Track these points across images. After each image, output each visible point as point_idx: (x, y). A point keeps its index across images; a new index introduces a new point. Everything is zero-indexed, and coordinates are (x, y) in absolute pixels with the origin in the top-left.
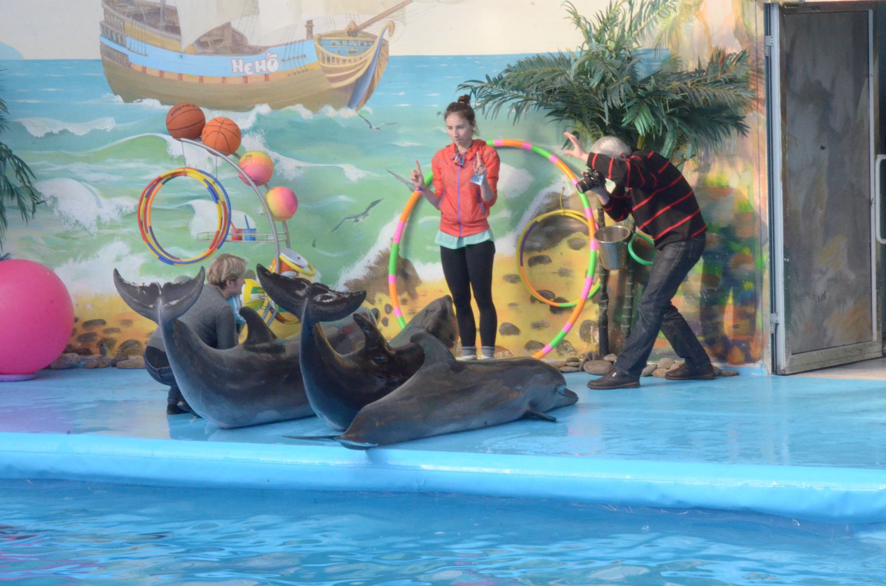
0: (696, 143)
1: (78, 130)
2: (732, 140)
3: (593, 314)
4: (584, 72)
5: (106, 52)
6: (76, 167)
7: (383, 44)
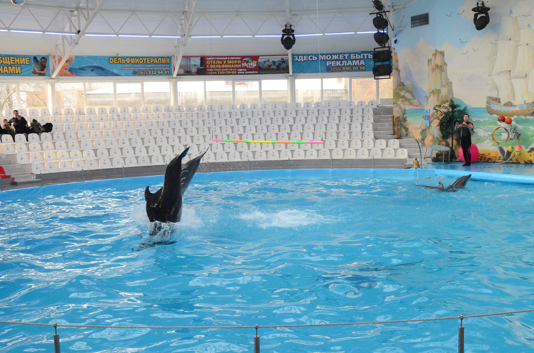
1: (481, 120)
5: (487, 106)
6: (481, 127)
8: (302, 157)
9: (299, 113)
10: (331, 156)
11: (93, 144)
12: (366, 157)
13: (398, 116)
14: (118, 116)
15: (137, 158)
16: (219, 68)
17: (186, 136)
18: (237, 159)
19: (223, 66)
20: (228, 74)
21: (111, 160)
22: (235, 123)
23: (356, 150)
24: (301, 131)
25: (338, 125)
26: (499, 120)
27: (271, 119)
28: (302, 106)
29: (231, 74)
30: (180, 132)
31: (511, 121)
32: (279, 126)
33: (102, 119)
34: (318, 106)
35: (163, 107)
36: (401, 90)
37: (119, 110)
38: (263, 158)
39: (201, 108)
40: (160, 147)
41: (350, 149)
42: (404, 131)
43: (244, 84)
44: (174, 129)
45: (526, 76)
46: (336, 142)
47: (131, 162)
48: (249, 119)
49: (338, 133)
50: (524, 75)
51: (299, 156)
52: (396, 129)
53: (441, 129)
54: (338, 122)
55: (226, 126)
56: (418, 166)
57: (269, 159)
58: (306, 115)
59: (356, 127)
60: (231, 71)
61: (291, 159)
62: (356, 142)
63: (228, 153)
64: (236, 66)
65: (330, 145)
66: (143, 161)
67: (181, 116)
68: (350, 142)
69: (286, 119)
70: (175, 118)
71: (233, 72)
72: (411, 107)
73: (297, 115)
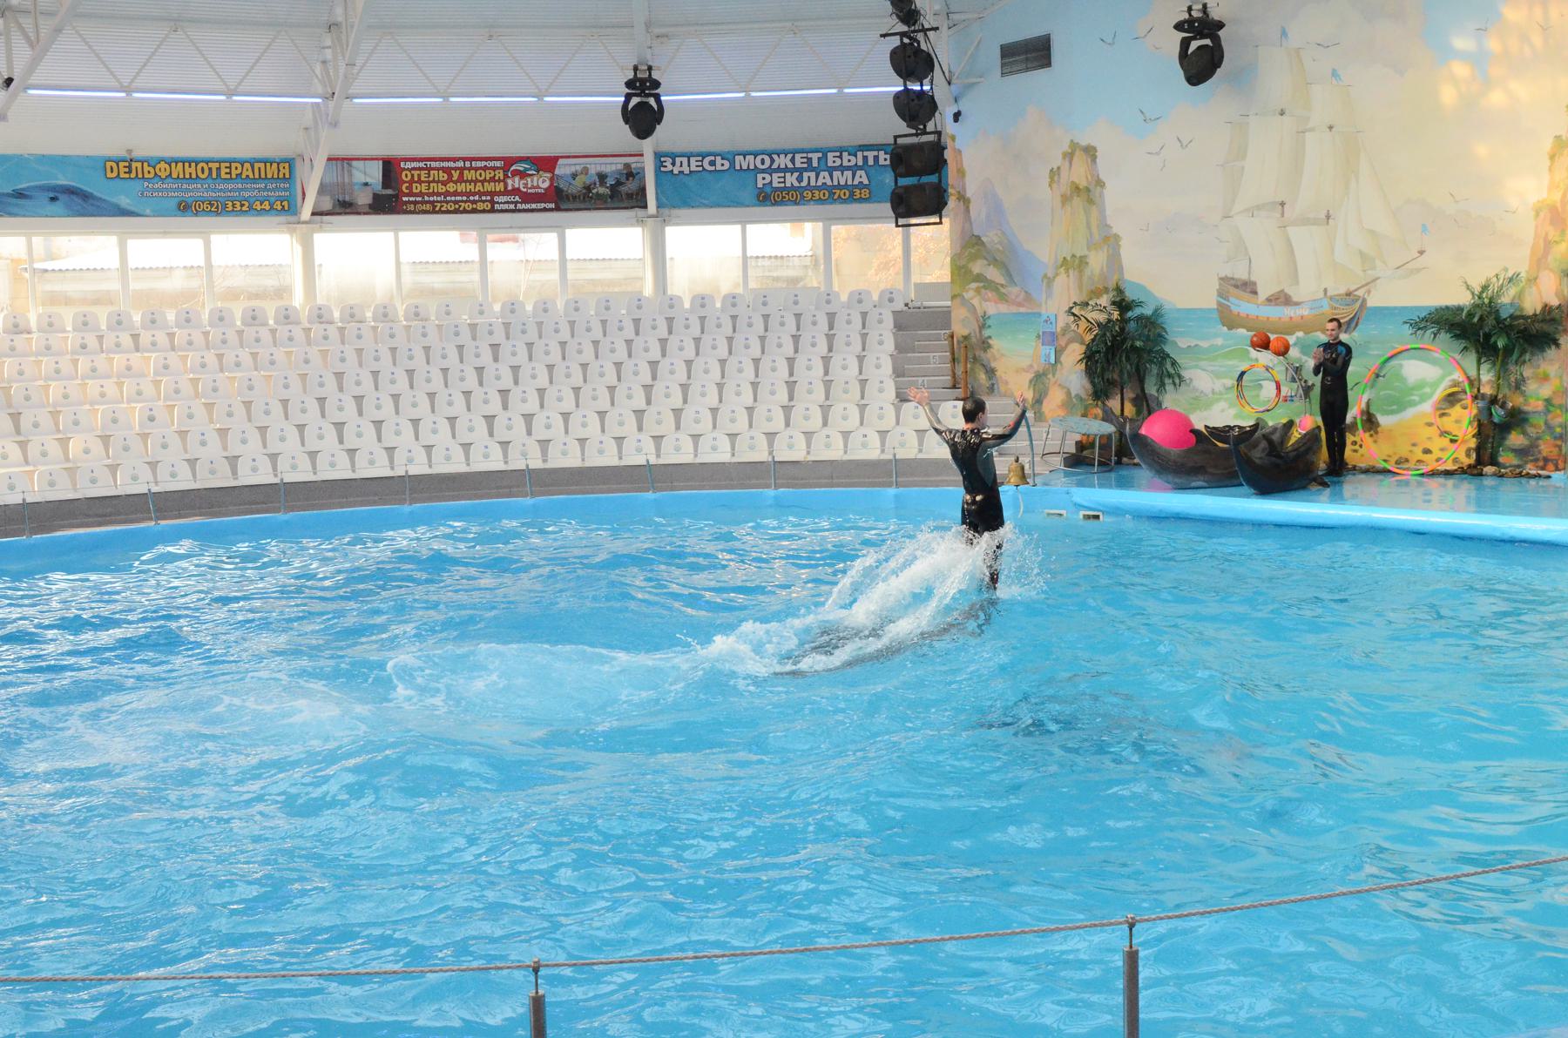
0: (1533, 354)
1: (1204, 344)
2: (1551, 352)
3: (1473, 443)
4: (1471, 315)
5: (1219, 304)
6: (1203, 363)
7: (1364, 300)
8: (687, 458)
9: (678, 325)
10: (771, 453)
11: (57, 424)
12: (873, 453)
13: (966, 333)
14: (135, 337)
15: (192, 463)
16: (439, 194)
17: (341, 396)
18: (495, 463)
19: (451, 187)
20: (465, 211)
21: (113, 469)
22: (486, 357)
23: (846, 435)
24: (684, 379)
25: (791, 361)
26: (1254, 345)
27: (596, 343)
28: (687, 305)
29: (474, 211)
30: (321, 385)
31: (1287, 349)
32: (618, 365)
33: (84, 347)
34: (734, 305)
35: (270, 309)
36: (973, 258)
37: (137, 318)
38: (572, 460)
39: (385, 314)
40: (263, 430)
41: (826, 431)
42: (982, 376)
43: (516, 240)
44: (303, 377)
45: (1328, 217)
46: (787, 410)
47: (173, 475)
48: (530, 345)
49: (791, 386)
50: (1323, 216)
51: (679, 452)
52: (960, 370)
53: (1090, 372)
54: (791, 353)
55: (461, 366)
56: (1023, 478)
57: (587, 464)
58: (697, 333)
59: (844, 368)
60: (474, 202)
61: (653, 461)
62: (846, 412)
63: (466, 447)
64: (489, 187)
65: (769, 420)
66: (213, 472)
67: (326, 338)
68: (825, 410)
69: (639, 343)
70: (309, 344)
71: (480, 206)
72: (1003, 308)
73: (670, 332)
